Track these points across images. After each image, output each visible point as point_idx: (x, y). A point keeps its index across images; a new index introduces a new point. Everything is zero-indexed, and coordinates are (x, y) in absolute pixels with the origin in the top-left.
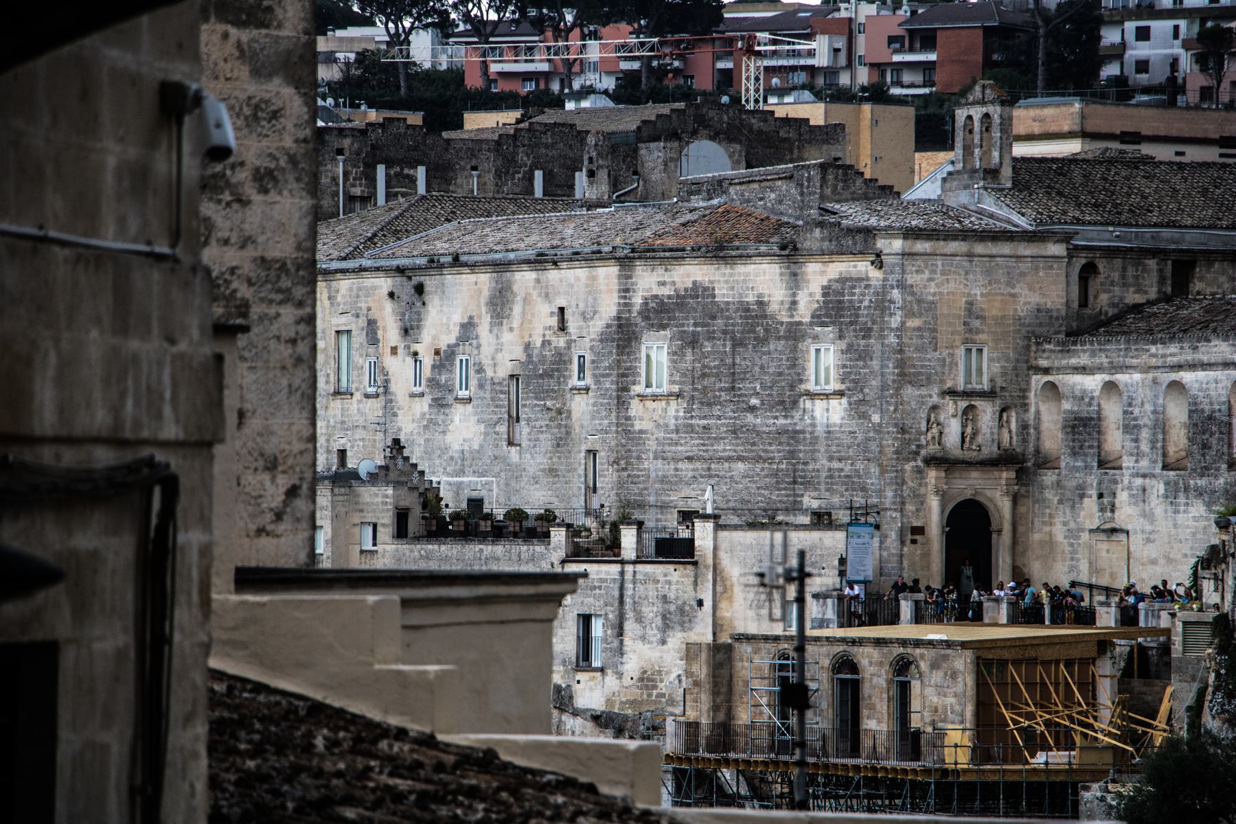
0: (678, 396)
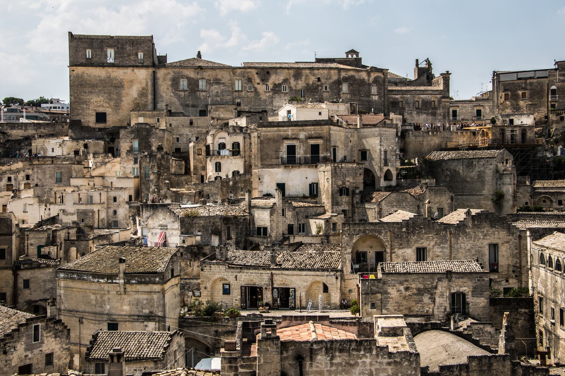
0: (350, 93)
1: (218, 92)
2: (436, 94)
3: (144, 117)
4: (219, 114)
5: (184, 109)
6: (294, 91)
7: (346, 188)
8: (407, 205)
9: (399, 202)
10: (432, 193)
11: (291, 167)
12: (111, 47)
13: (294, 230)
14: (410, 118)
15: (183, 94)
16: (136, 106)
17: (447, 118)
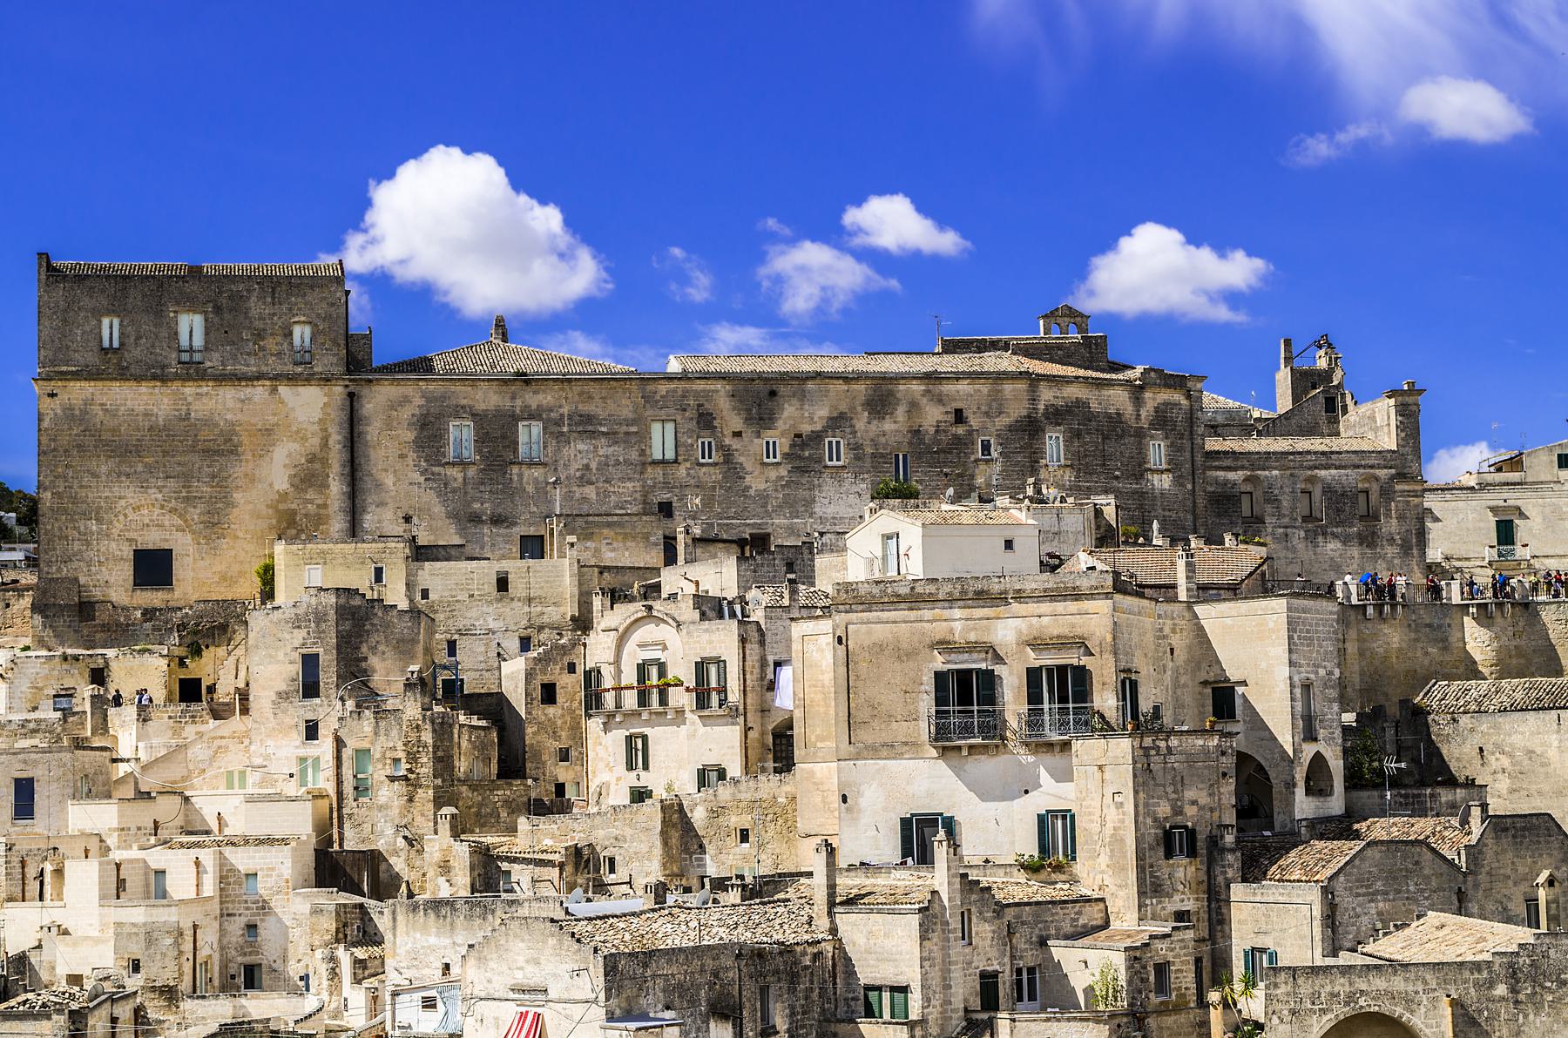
0: (1071, 466)
1: (587, 467)
2: (1372, 467)
3: (325, 563)
4: (597, 550)
5: (462, 531)
6: (868, 460)
7: (1186, 827)
8: (1422, 891)
9: (1395, 878)
10: (1506, 840)
11: (965, 752)
12: (192, 305)
13: (1001, 994)
14: (1282, 554)
15: (460, 476)
16: (284, 525)
17: (1415, 552)
